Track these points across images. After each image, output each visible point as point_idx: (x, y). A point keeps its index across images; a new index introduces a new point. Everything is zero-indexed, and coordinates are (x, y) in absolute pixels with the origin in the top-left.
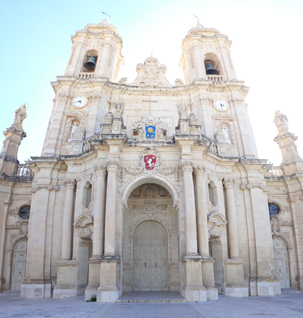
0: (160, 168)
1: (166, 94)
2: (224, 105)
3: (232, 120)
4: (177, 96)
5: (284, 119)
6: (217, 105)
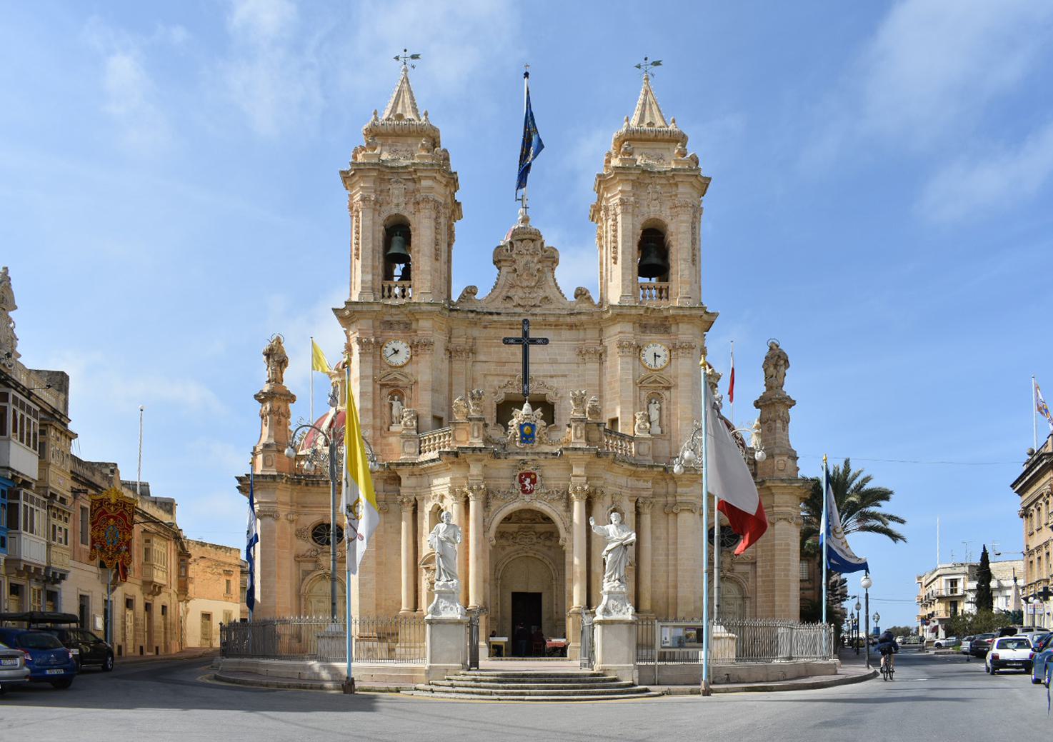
0: (543, 491)
1: (556, 326)
2: (659, 356)
3: (668, 388)
4: (578, 330)
5: (782, 362)
6: (648, 356)
